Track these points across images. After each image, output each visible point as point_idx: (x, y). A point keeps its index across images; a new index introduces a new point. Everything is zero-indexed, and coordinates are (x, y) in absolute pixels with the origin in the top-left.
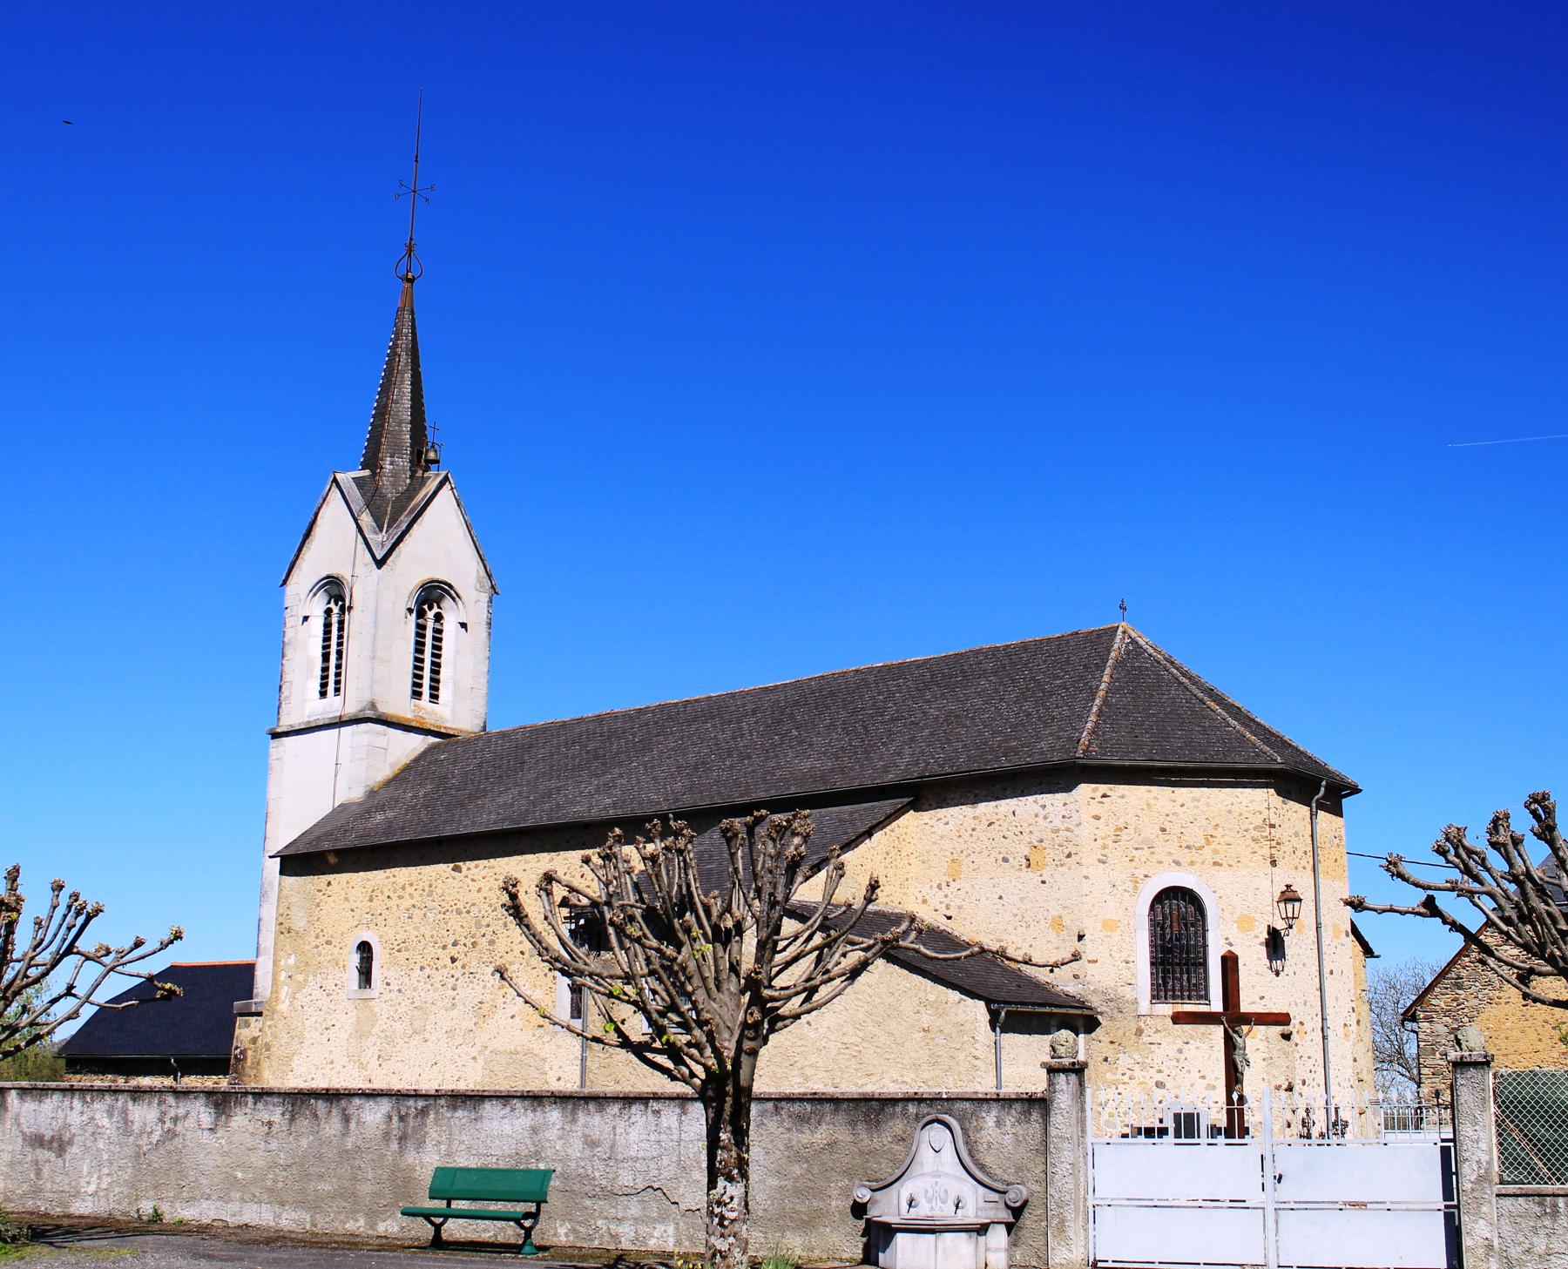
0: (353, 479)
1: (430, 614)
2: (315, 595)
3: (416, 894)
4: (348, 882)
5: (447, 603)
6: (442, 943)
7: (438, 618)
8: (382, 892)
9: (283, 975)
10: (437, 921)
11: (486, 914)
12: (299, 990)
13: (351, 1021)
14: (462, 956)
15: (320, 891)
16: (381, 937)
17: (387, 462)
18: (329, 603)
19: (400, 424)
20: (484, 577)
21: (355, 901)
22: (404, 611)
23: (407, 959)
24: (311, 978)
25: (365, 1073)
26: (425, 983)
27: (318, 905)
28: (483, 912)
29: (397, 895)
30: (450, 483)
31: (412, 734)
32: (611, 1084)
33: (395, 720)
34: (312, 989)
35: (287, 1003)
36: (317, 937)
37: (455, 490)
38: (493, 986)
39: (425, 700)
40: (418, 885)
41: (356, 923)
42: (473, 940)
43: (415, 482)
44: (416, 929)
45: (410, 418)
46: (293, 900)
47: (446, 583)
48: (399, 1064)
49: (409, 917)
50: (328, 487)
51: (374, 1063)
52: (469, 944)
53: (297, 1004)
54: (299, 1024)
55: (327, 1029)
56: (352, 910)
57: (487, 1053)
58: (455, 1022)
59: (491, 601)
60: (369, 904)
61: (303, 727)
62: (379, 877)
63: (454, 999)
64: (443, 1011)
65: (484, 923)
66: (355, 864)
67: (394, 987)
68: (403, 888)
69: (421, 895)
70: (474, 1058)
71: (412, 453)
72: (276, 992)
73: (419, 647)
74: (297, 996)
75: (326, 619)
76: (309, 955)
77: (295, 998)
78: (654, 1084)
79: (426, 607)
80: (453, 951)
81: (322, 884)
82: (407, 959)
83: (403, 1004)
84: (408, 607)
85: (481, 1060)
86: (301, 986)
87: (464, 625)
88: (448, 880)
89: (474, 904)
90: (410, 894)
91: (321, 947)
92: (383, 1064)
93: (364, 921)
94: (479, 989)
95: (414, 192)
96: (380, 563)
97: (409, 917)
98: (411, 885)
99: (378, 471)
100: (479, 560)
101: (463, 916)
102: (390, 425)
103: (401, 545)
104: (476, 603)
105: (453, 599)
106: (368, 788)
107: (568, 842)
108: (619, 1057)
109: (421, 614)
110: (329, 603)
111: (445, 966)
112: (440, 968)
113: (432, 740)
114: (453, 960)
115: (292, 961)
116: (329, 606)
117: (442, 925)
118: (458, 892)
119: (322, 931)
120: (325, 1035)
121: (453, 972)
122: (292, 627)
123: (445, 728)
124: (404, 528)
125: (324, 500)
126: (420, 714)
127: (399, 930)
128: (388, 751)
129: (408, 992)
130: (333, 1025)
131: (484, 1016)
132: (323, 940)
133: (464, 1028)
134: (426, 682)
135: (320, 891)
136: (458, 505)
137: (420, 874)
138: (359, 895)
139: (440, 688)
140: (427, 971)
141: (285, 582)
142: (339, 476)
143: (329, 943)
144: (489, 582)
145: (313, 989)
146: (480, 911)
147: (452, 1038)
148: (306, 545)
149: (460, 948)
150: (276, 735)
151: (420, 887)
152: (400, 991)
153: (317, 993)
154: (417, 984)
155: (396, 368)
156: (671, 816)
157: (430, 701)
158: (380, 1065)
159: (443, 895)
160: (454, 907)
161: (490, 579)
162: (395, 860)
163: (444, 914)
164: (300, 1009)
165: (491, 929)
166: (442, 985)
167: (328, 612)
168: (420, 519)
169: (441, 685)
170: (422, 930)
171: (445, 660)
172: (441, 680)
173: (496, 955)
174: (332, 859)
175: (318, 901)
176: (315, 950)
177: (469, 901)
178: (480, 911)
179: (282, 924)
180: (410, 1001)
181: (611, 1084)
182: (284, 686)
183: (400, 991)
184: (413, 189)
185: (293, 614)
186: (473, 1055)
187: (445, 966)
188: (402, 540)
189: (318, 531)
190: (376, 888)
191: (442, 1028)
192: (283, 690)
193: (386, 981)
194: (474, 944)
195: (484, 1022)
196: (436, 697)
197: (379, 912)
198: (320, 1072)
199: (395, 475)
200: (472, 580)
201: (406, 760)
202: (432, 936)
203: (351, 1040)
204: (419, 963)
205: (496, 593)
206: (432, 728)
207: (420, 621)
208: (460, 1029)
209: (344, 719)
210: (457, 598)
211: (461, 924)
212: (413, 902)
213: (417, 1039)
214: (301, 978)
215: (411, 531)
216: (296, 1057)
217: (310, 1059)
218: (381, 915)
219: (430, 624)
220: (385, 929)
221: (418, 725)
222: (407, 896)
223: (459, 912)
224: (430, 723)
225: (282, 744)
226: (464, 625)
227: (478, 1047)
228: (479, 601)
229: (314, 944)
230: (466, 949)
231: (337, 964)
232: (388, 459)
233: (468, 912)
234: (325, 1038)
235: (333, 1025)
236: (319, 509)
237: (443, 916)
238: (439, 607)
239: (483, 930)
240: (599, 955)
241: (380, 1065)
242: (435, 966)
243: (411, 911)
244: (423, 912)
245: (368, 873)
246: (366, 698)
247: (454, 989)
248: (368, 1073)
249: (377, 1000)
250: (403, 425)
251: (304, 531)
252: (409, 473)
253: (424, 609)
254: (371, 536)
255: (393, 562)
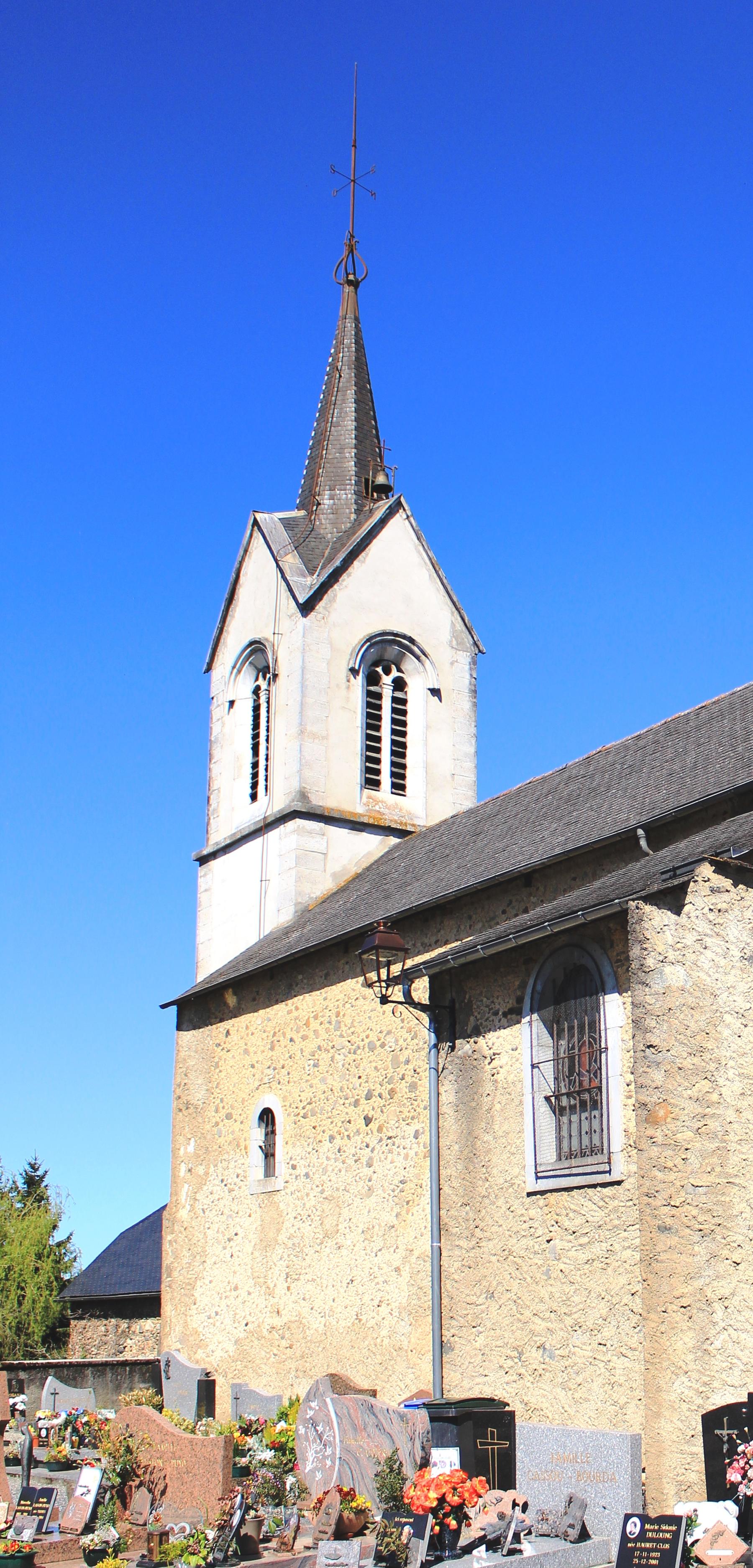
0: (280, 519)
1: (387, 680)
2: (239, 672)
3: (322, 1032)
4: (247, 1028)
5: (410, 664)
6: (353, 1097)
7: (399, 684)
8: (284, 1034)
9: (183, 1168)
10: (347, 1066)
11: (404, 1045)
12: (200, 1188)
13: (254, 1226)
14: (376, 1114)
15: (219, 1045)
16: (285, 1099)
17: (326, 497)
18: (257, 679)
19: (341, 450)
20: (462, 632)
21: (255, 1053)
22: (344, 672)
23: (314, 1128)
24: (212, 1169)
25: (272, 1301)
26: (336, 1160)
27: (217, 1065)
28: (401, 1042)
29: (300, 1035)
30: (404, 510)
31: (364, 834)
32: (480, 1301)
33: (336, 815)
34: (213, 1185)
35: (188, 1207)
36: (217, 1111)
37: (412, 519)
38: (416, 1154)
39: (385, 791)
40: (323, 1016)
41: (257, 1084)
42: (389, 1087)
43: (361, 516)
44: (323, 1080)
45: (354, 441)
46: (191, 1063)
47: (404, 637)
48: (309, 1286)
49: (315, 1066)
50: (249, 532)
51: (282, 1286)
52: (386, 1095)
53: (199, 1206)
54: (201, 1236)
55: (230, 1240)
56: (253, 1066)
57: (413, 1259)
58: (373, 1215)
59: (474, 662)
60: (271, 1053)
61: (228, 842)
62: (280, 1014)
63: (370, 1180)
64: (358, 1200)
65: (402, 1059)
66: (254, 1000)
67: (301, 1171)
68: (307, 1024)
69: (327, 1030)
70: (397, 1269)
71: (357, 483)
72: (176, 1195)
73: (372, 720)
74: (198, 1196)
75: (255, 700)
76: (209, 1137)
77: (195, 1199)
78: (551, 1296)
79: (379, 670)
80: (366, 1107)
81: (221, 1036)
82: (314, 1128)
83: (311, 1195)
84: (350, 666)
85: (406, 1274)
86: (202, 1181)
87: (435, 692)
88: (358, 1002)
89: (389, 1032)
90: (314, 1031)
91: (221, 1124)
92: (292, 1286)
93: (266, 1080)
94: (400, 1161)
95: (354, 181)
96: (306, 608)
97: (315, 1066)
98: (316, 1017)
99: (315, 508)
100: (454, 609)
101: (376, 1052)
102: (331, 453)
103: (336, 587)
104: (452, 663)
105: (418, 658)
106: (300, 907)
107: (504, 912)
108: (491, 1245)
109: (373, 679)
110: (257, 679)
111: (358, 1132)
112: (352, 1135)
113: (393, 841)
114: (368, 1120)
115: (191, 1149)
116: (257, 683)
117: (353, 1069)
118: (370, 1018)
119: (222, 1100)
120: (228, 1248)
121: (367, 1140)
122: (219, 720)
123: (413, 825)
124: (337, 563)
125: (246, 551)
126: (377, 808)
127: (304, 1085)
128: (329, 856)
129: (317, 1176)
130: (236, 1234)
131: (408, 1203)
132: (223, 1113)
133: (383, 1225)
134: (385, 767)
135: (219, 1045)
136: (418, 539)
137: (325, 999)
138: (260, 1043)
139: (407, 775)
140: (338, 1141)
141: (209, 668)
142: (259, 516)
143: (229, 1116)
144: (470, 637)
145: (214, 1185)
146: (397, 1041)
147: (370, 1240)
148: (230, 613)
149: (376, 1101)
150: (203, 860)
151: (326, 1019)
152: (307, 1175)
153: (219, 1191)
154: (326, 1162)
155: (336, 385)
156: (640, 832)
157: (392, 793)
158: (288, 1288)
159: (352, 1025)
160: (367, 1041)
161: (470, 633)
162: (297, 985)
163: (355, 1053)
164: (202, 1214)
165: (411, 1067)
166: (356, 1161)
167: (256, 691)
168: (363, 554)
169: (408, 773)
170: (330, 1081)
171: (412, 739)
172: (408, 765)
173: (418, 1106)
174: (231, 1000)
175: (216, 1059)
176: (215, 1129)
177: (384, 1028)
178: (397, 1041)
179: (179, 1097)
180: (320, 1188)
181: (481, 1300)
182: (212, 797)
183: (307, 1175)
184: (352, 178)
185: (220, 703)
186: (396, 1264)
187: (358, 1132)
188: (337, 581)
189: (242, 593)
190: (277, 1030)
191: (357, 1227)
192: (211, 802)
193: (291, 1162)
194: (392, 1092)
195: (408, 1212)
196: (403, 787)
197: (282, 1062)
198: (223, 1303)
199: (335, 511)
200: (445, 634)
201: (355, 869)
202: (342, 1089)
203: (257, 1254)
204: (327, 1131)
205: (480, 651)
206: (394, 826)
207: (372, 688)
208: (380, 1225)
209: (269, 820)
210: (423, 657)
211: (374, 1064)
212: (319, 1041)
213: (329, 1245)
214: (201, 1170)
215: (350, 570)
216: (199, 1283)
217: (213, 1284)
218: (283, 1067)
219: (387, 693)
220: (289, 1087)
221: (371, 821)
222: (311, 1035)
223: (372, 1048)
224: (390, 819)
225: (210, 870)
226: (435, 692)
227: (401, 1252)
228: (457, 661)
229: (214, 1120)
230: (382, 1102)
231: (238, 1145)
232: (327, 493)
233: (383, 1045)
234: (228, 1252)
235: (236, 1234)
236: (241, 563)
237: (354, 1057)
238: (399, 670)
239: (401, 1070)
240: (453, 1048)
241: (288, 1288)
242: (346, 1133)
243: (317, 1056)
244: (330, 1055)
245: (268, 1010)
246: (295, 785)
247: (370, 1165)
248: (276, 1300)
249: (283, 1193)
250: (346, 450)
251: (226, 596)
252: (354, 507)
253: (377, 672)
254: (295, 579)
255: (325, 608)
